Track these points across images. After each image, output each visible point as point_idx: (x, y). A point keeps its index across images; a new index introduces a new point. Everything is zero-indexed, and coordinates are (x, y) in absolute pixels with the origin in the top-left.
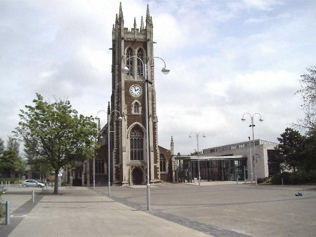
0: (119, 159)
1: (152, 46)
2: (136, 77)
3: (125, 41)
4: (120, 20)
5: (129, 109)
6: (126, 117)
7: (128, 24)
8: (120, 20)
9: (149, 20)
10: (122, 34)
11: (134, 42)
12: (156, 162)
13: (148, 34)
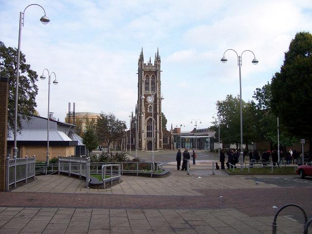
0: (140, 137)
1: (160, 73)
2: (150, 92)
3: (145, 72)
4: (141, 59)
5: (146, 110)
6: (145, 114)
7: (146, 61)
8: (141, 59)
9: (158, 59)
10: (143, 67)
11: (150, 72)
12: (160, 138)
13: (158, 67)
